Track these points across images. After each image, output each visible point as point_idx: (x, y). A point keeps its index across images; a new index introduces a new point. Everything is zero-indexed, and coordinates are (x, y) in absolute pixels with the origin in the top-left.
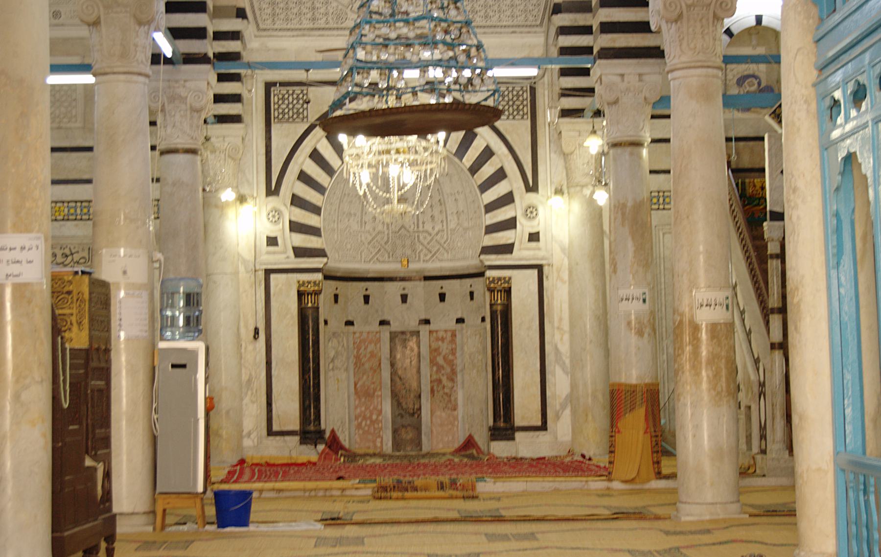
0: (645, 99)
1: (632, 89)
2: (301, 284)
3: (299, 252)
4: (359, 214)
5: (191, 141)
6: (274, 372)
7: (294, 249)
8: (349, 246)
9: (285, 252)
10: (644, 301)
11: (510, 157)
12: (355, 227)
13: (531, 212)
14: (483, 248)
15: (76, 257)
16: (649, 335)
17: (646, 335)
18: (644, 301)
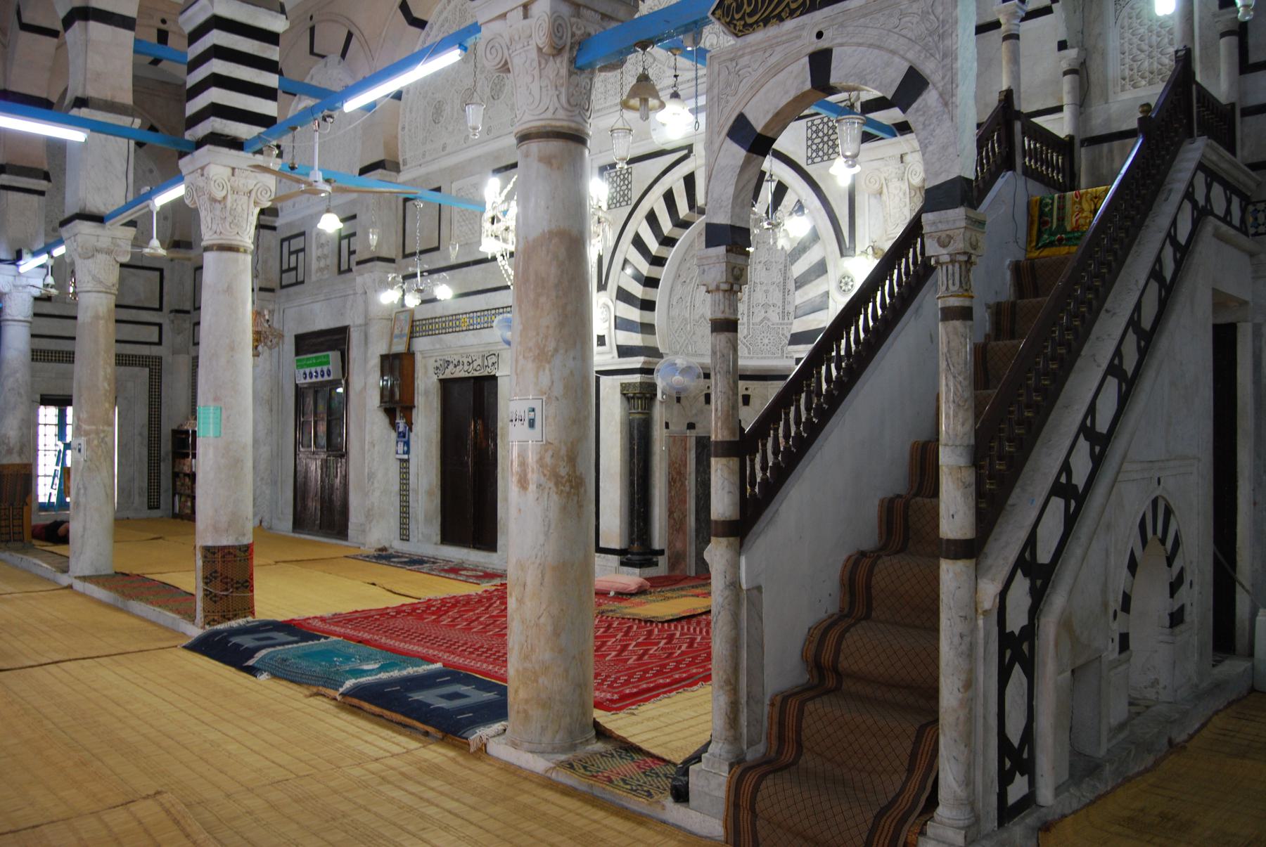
0: (540, 50)
1: (516, 38)
2: (624, 387)
3: (624, 351)
4: (780, 304)
5: (215, 236)
6: (601, 484)
7: (619, 347)
8: (766, 341)
9: (610, 352)
10: (532, 424)
11: (823, 212)
12: (774, 316)
13: (846, 284)
14: (792, 335)
15: (475, 364)
16: (539, 486)
17: (532, 487)
18: (532, 424)
